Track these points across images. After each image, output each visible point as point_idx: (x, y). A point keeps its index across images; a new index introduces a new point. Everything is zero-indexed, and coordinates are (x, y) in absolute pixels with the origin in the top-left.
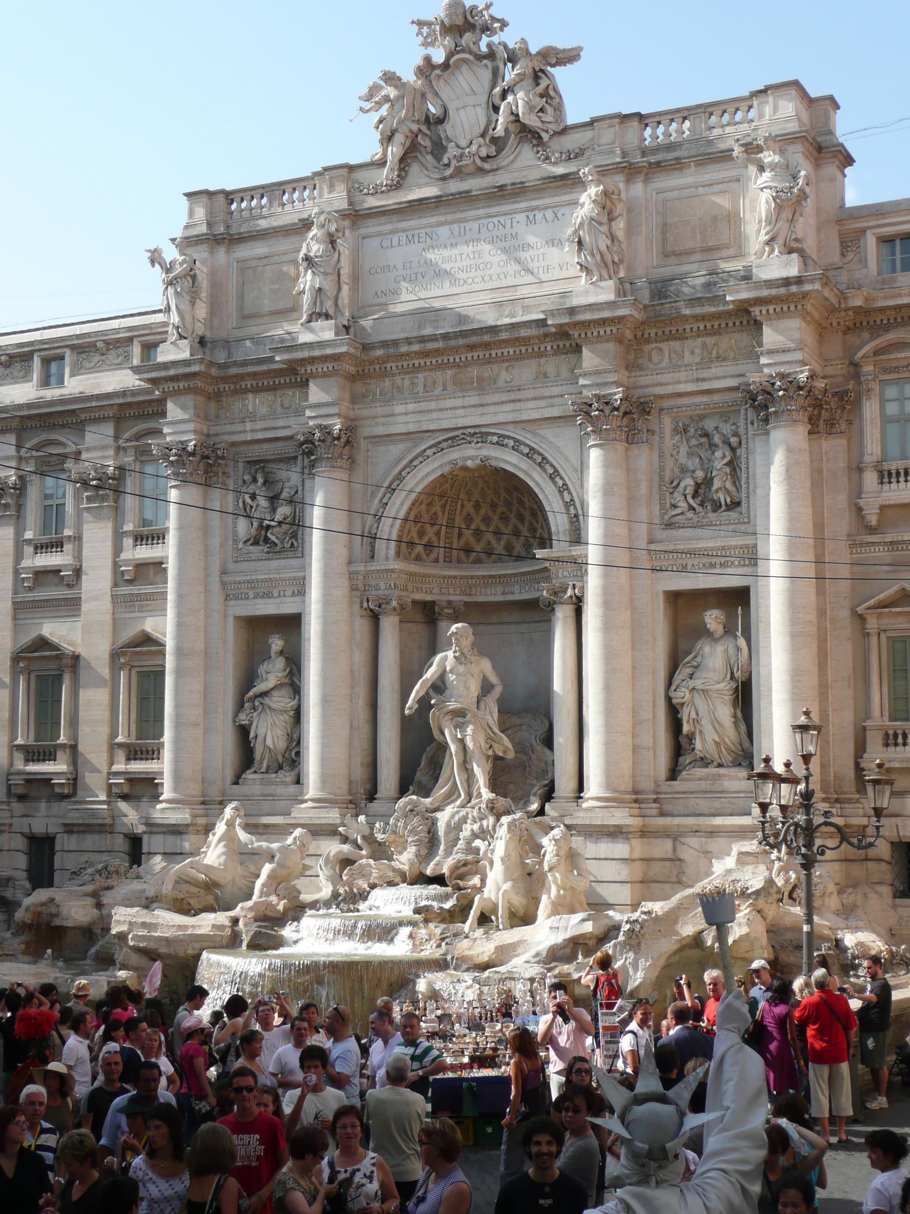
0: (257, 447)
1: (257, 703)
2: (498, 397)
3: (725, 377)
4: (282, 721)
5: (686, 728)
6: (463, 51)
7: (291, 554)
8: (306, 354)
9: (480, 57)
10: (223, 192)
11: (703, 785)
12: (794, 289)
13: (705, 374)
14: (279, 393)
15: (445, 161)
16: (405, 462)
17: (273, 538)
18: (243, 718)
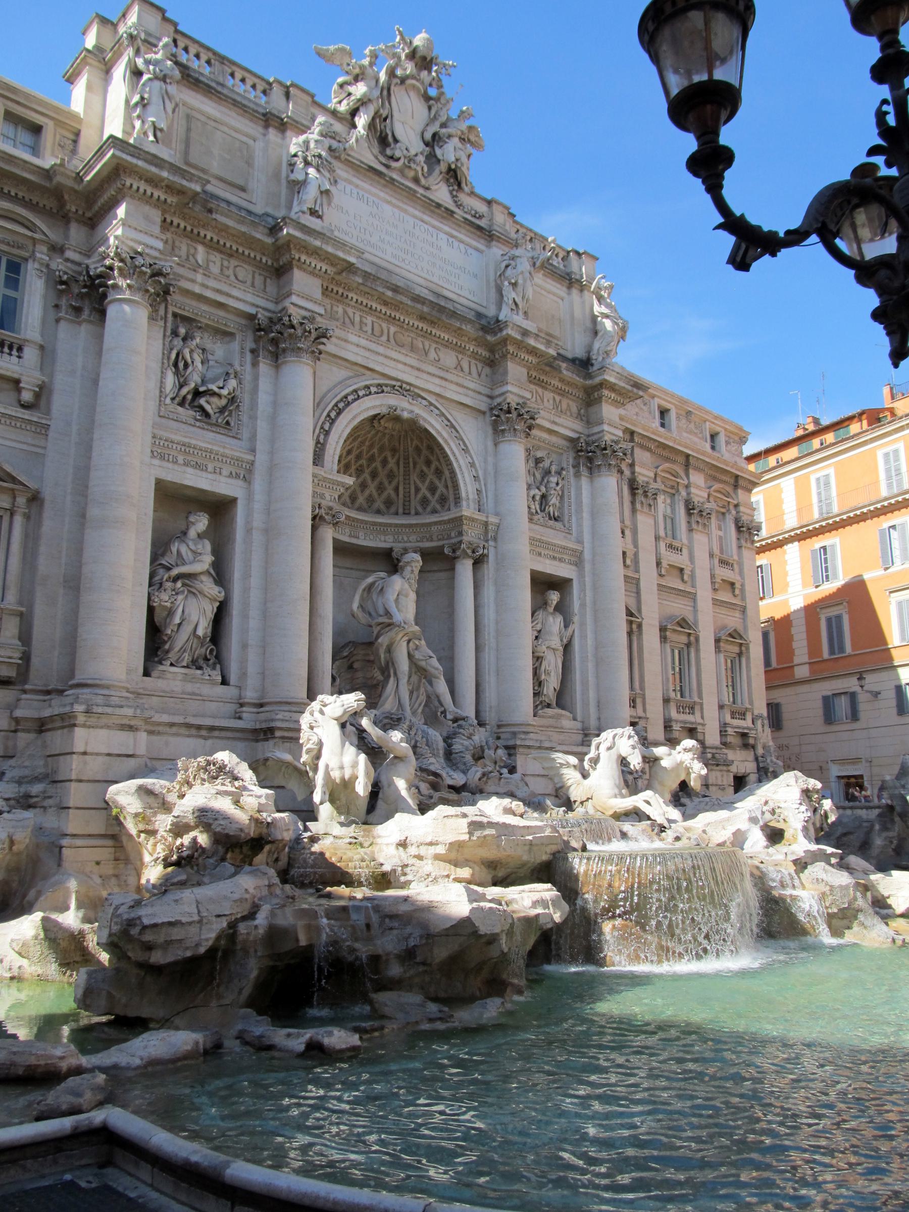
0: (194, 303)
1: (179, 584)
2: (431, 369)
3: (566, 428)
4: (210, 610)
5: (543, 677)
6: (418, 80)
7: (226, 431)
8: (318, 243)
9: (427, 98)
10: (175, 25)
11: (551, 722)
12: (635, 390)
13: (557, 420)
14: (234, 262)
15: (398, 154)
16: (351, 389)
17: (208, 408)
18: (164, 598)
